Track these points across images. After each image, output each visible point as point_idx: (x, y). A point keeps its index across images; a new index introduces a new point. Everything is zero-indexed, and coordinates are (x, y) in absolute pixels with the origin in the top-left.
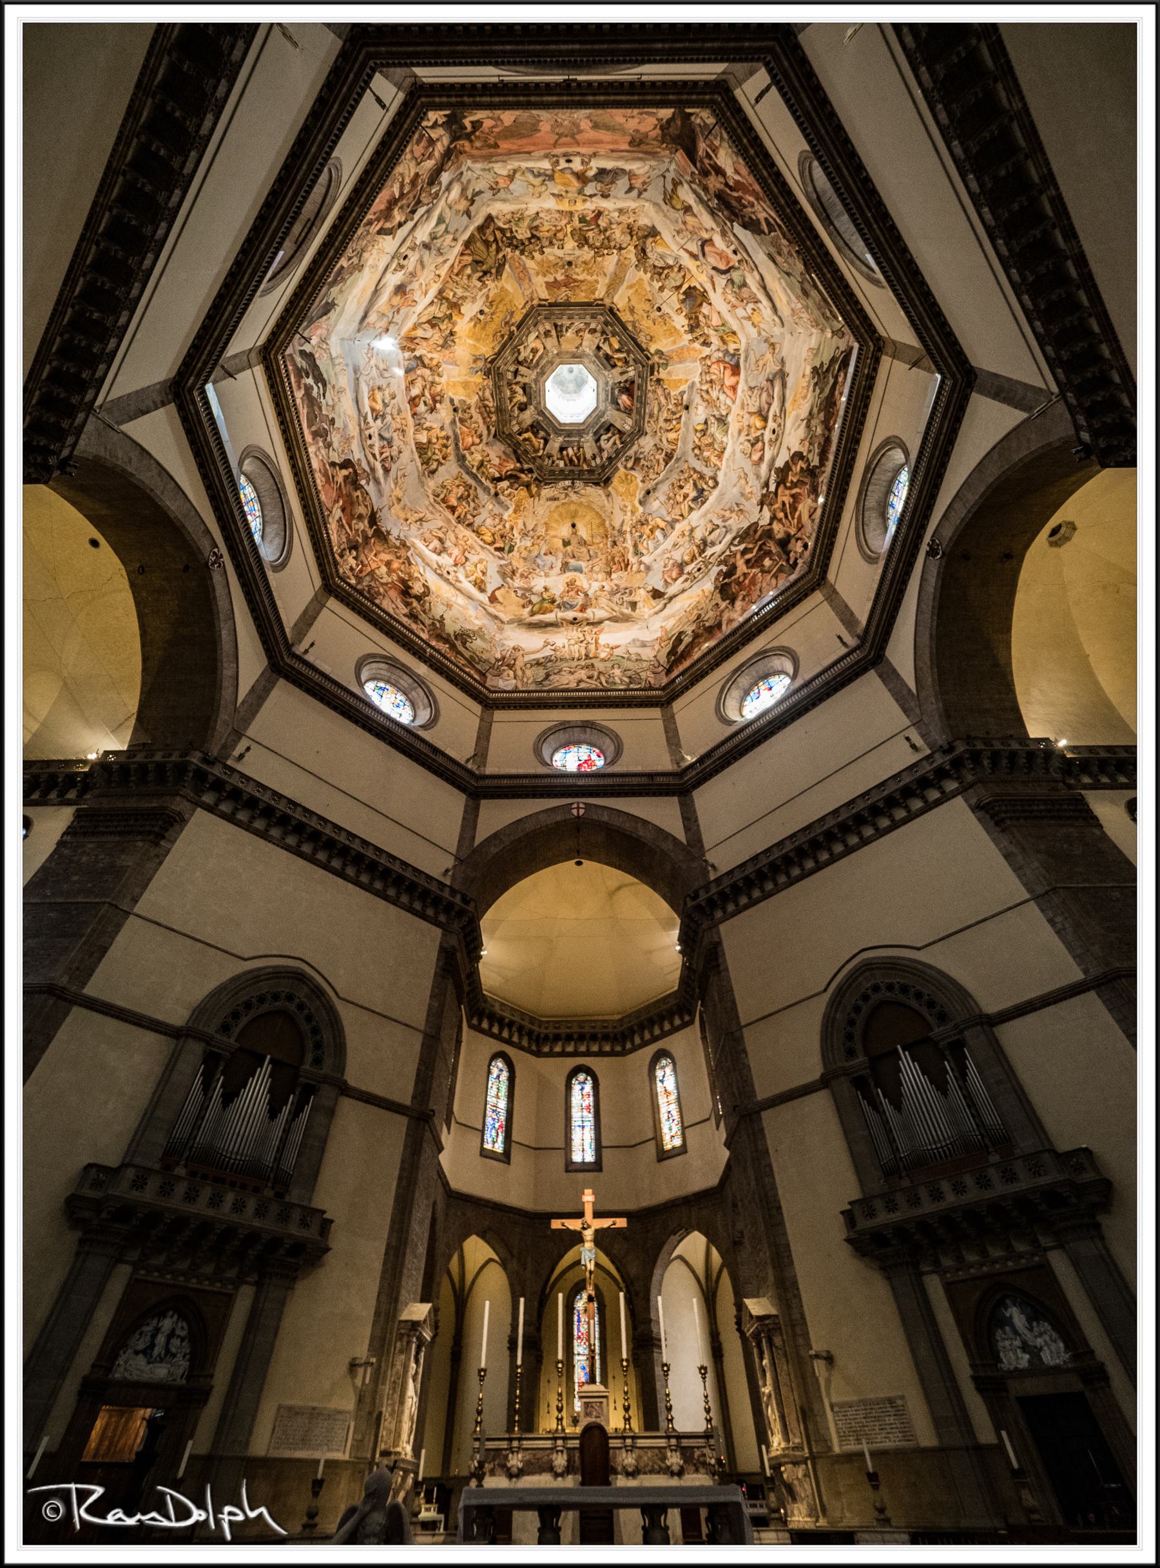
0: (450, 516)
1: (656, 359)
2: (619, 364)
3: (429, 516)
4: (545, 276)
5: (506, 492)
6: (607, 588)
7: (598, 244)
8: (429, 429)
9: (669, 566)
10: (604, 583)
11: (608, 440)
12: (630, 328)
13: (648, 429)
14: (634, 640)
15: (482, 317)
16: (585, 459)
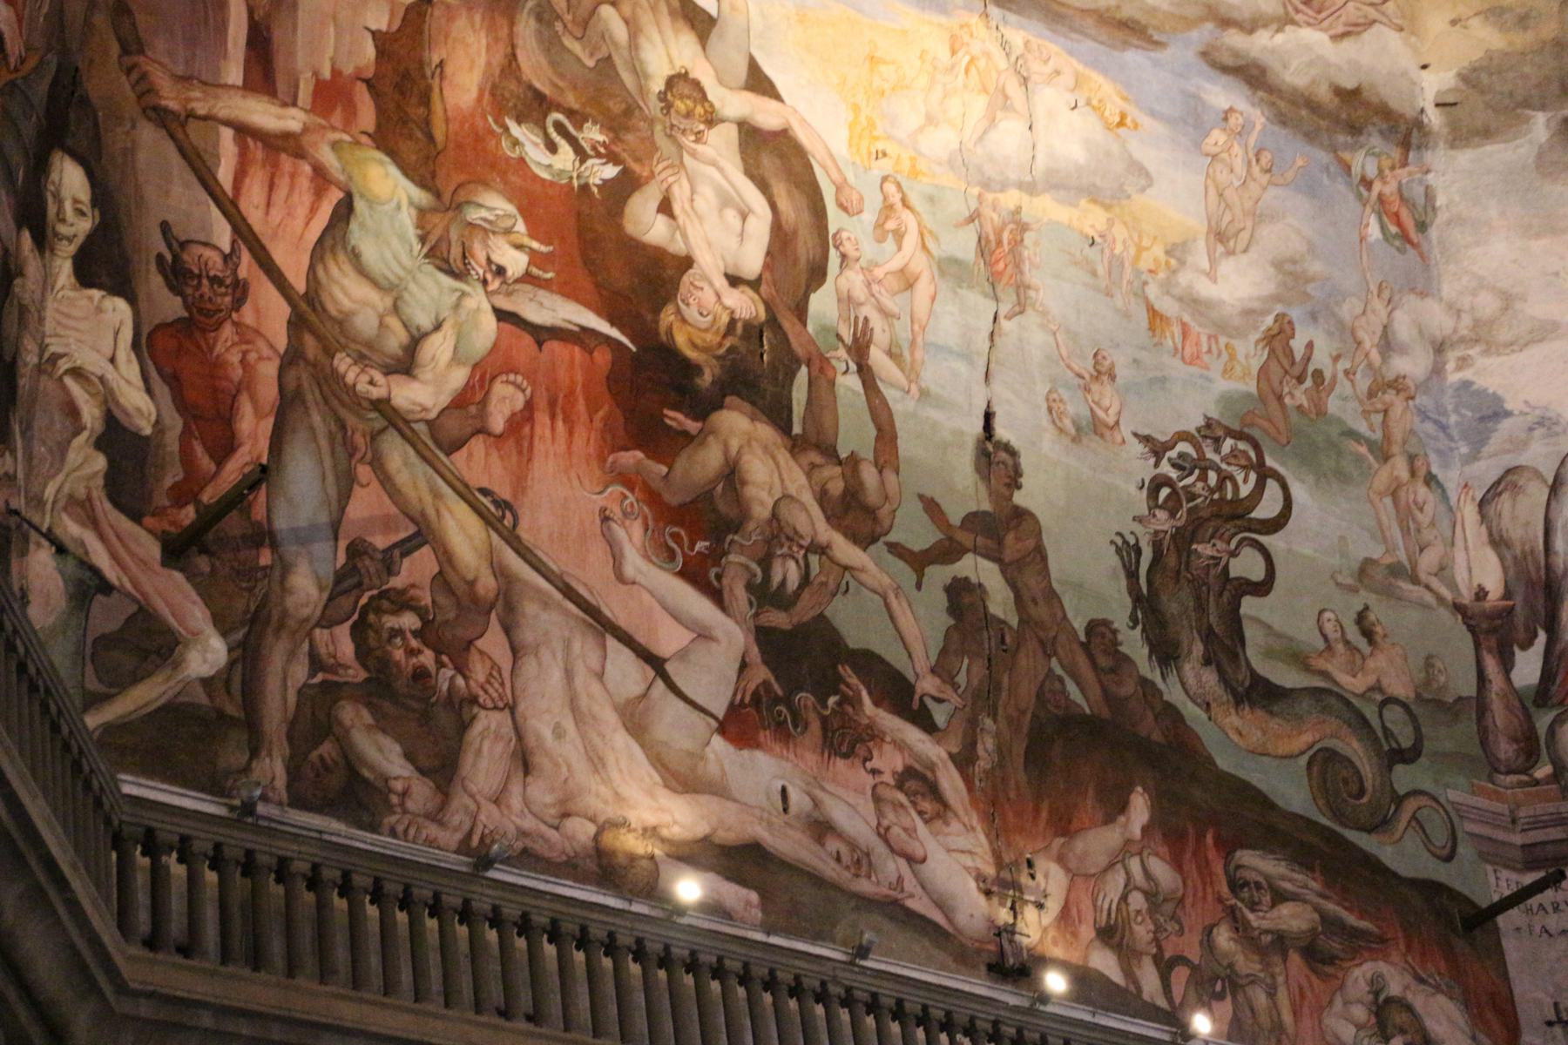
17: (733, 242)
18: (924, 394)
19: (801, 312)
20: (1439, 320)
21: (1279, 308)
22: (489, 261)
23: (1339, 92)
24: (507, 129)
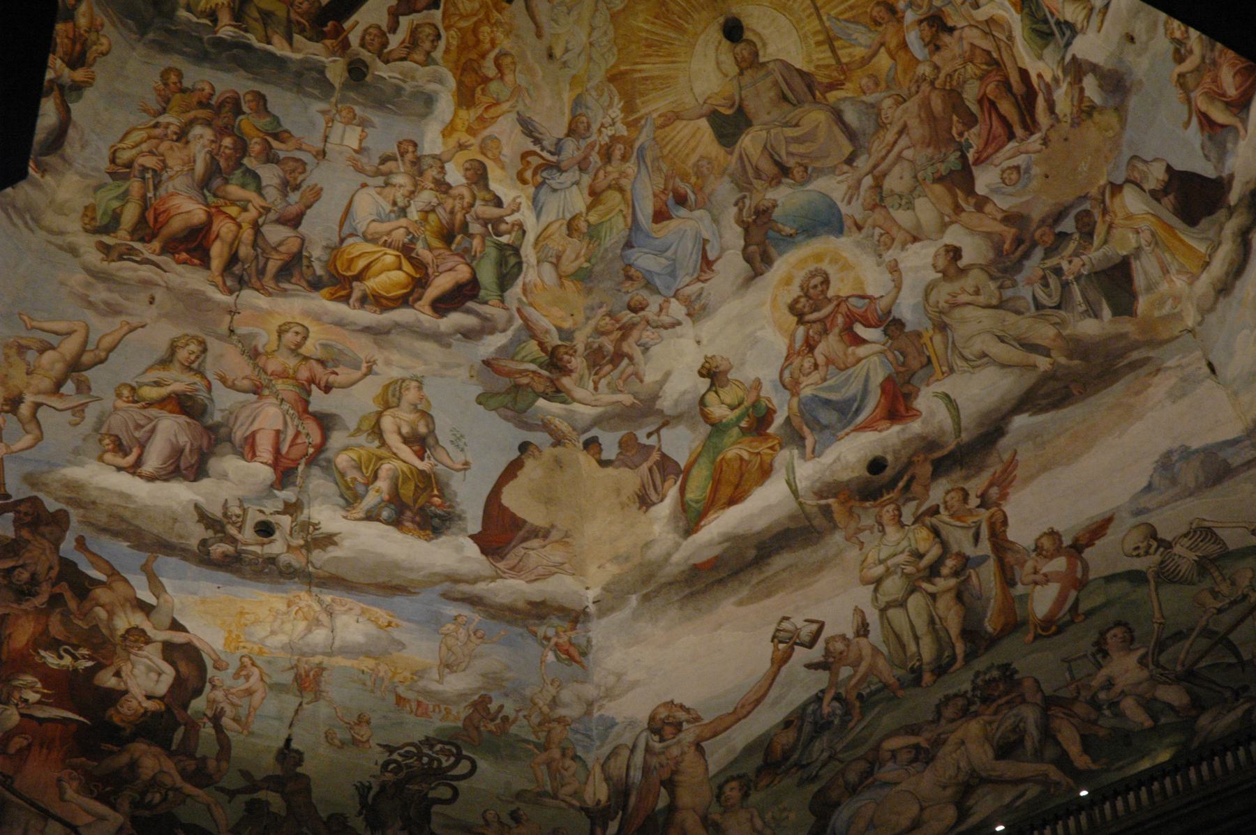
3: (103, 328)
5: (395, 41)
6: (973, 251)
9: (1197, 50)
10: (953, 236)
14: (1166, 464)
17: (152, 684)
18: (251, 734)
19: (185, 707)
20: (590, 691)
21: (483, 692)
22: (21, 698)
23: (531, 603)
24: (38, 653)
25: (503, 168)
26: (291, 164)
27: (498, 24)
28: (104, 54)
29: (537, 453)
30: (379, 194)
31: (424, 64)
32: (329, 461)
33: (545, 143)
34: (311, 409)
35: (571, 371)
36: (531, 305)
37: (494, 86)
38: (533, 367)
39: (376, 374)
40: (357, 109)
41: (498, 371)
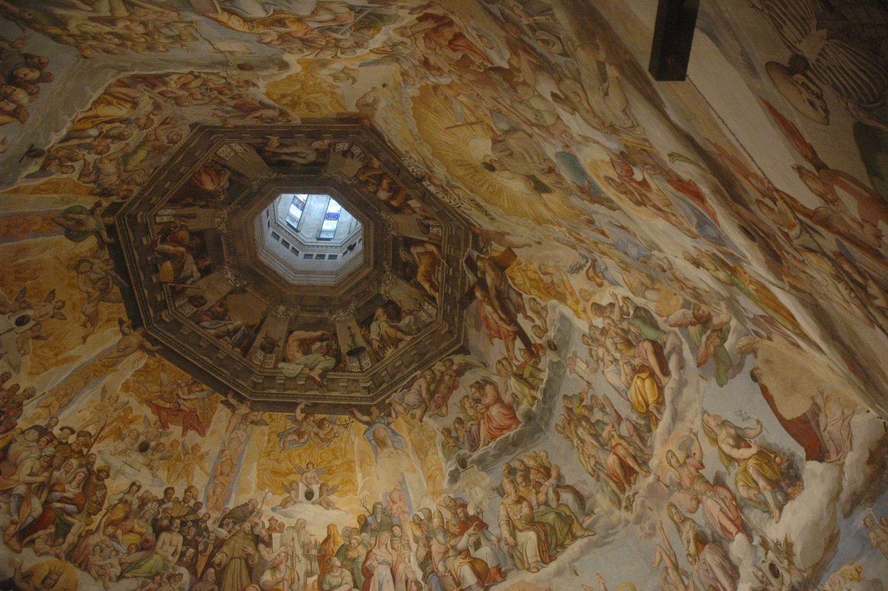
0: (643, 483)
1: (92, 223)
2: (183, 234)
4: (196, 447)
5: (538, 322)
7: (74, 462)
8: (513, 529)
11: (295, 154)
12: (116, 290)
13: (185, 133)
15: (315, 488)
16: (367, 167)
25: (595, 293)
26: (593, 401)
27: (526, 265)
28: (547, 457)
29: (759, 371)
30: (607, 367)
31: (547, 314)
32: (742, 499)
33: (583, 262)
34: (711, 482)
35: (709, 314)
36: (668, 316)
37: (556, 281)
38: (704, 338)
39: (697, 432)
40: (569, 355)
41: (705, 362)
